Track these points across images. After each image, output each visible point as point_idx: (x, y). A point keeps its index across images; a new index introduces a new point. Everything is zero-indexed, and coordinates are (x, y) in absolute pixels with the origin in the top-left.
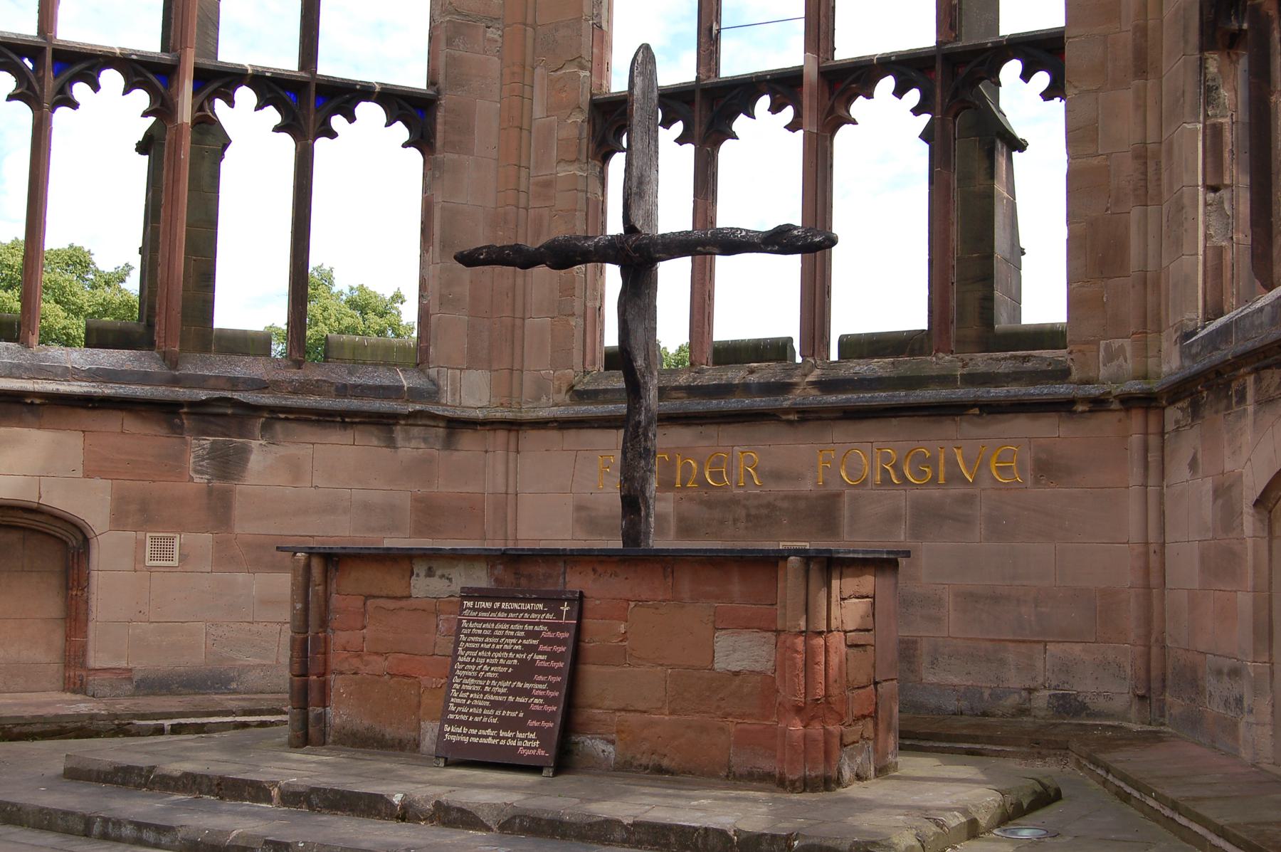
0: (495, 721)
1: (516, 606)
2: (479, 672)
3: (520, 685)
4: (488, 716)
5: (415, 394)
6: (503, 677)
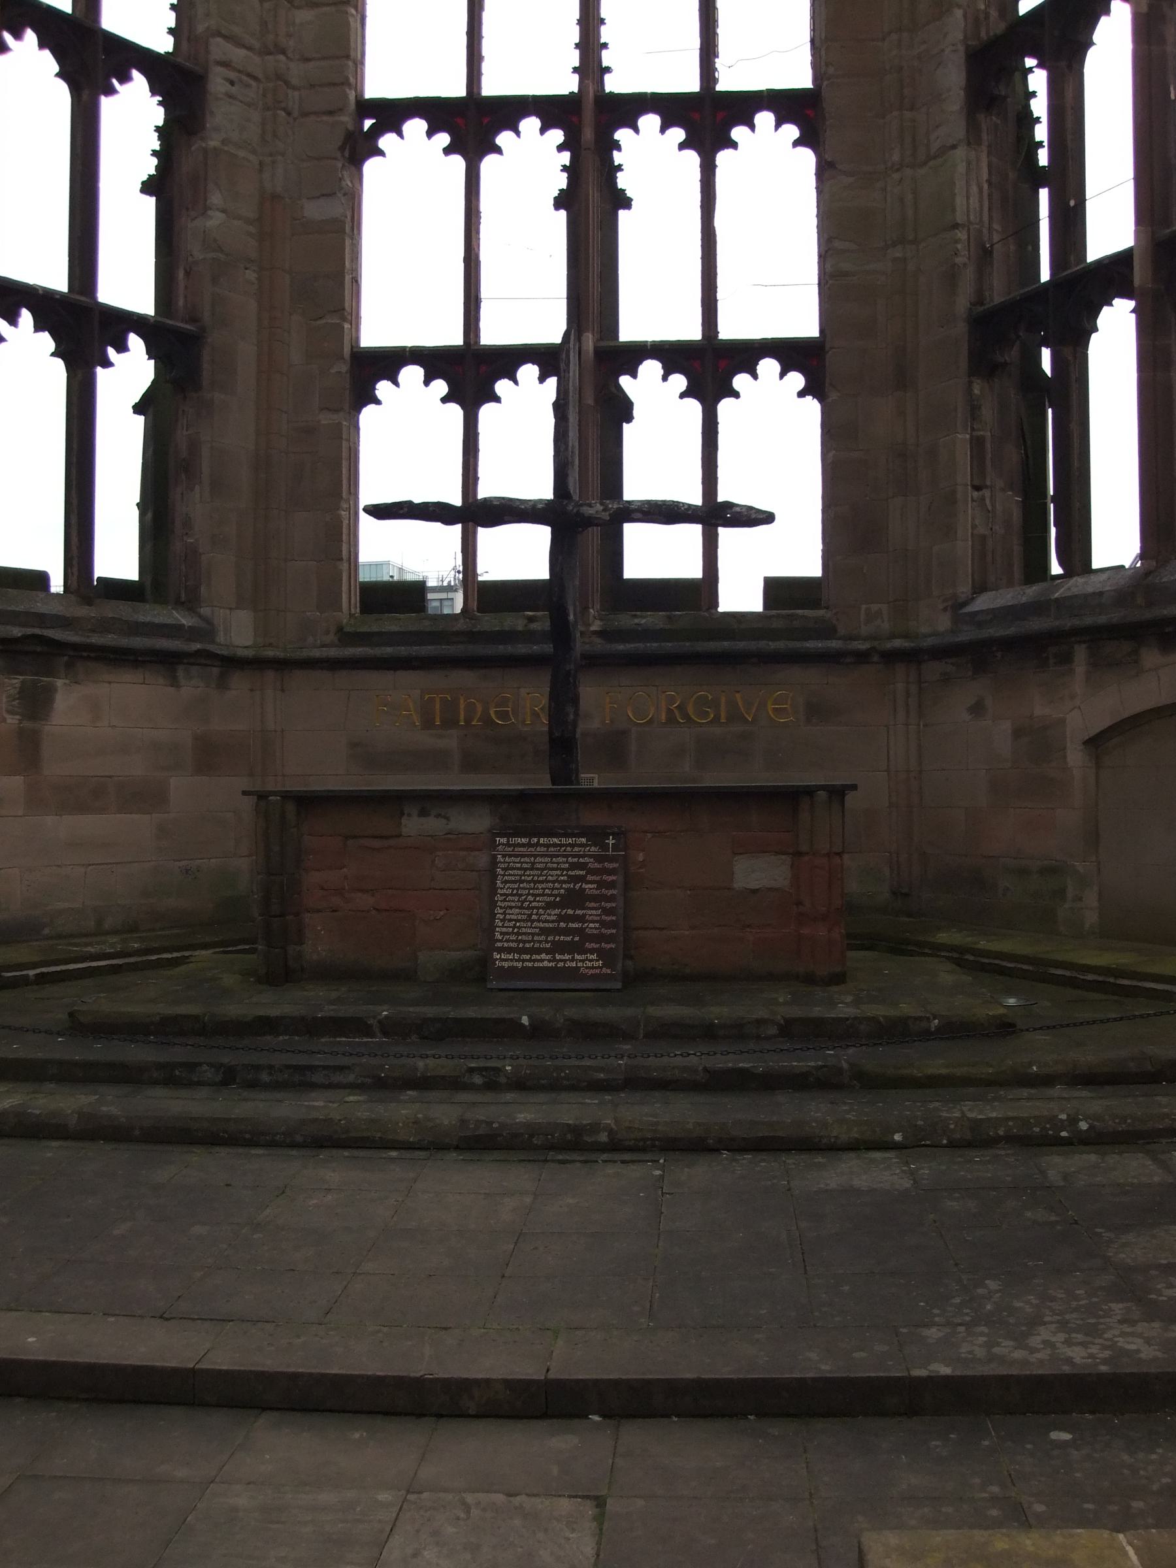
0: (548, 946)
1: (556, 840)
2: (523, 902)
3: (570, 912)
4: (540, 942)
5: (193, 634)
6: (549, 906)
